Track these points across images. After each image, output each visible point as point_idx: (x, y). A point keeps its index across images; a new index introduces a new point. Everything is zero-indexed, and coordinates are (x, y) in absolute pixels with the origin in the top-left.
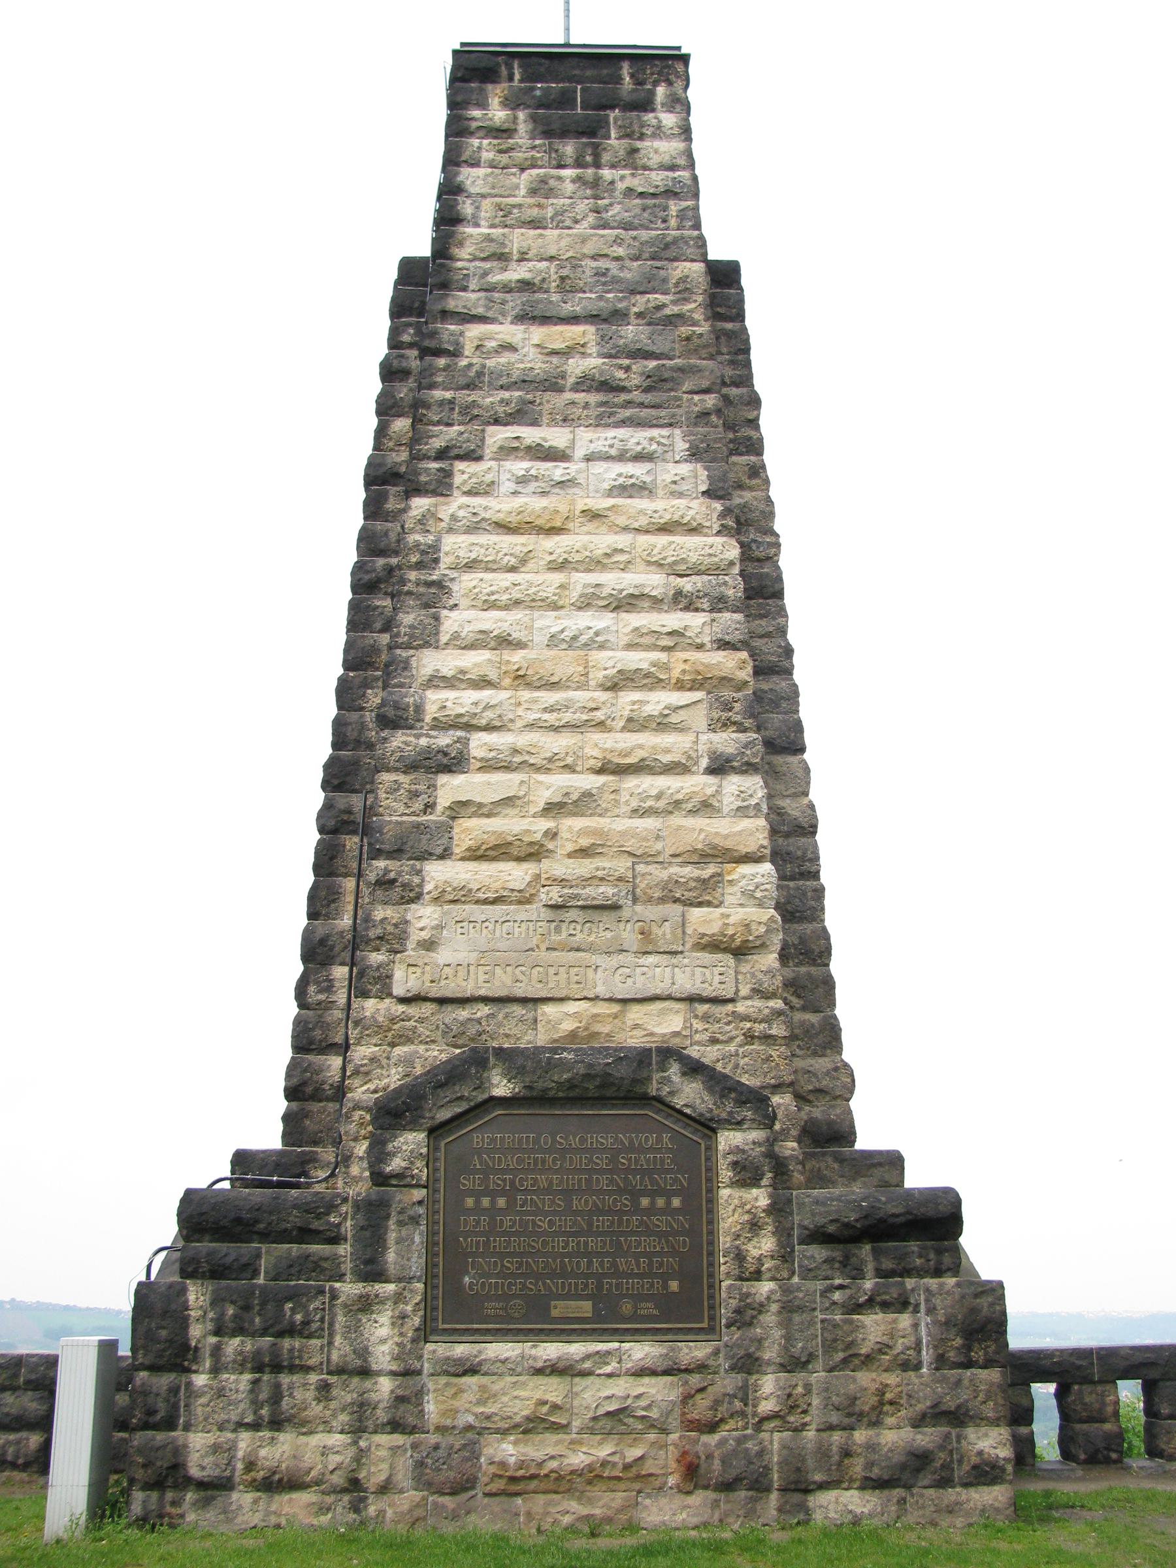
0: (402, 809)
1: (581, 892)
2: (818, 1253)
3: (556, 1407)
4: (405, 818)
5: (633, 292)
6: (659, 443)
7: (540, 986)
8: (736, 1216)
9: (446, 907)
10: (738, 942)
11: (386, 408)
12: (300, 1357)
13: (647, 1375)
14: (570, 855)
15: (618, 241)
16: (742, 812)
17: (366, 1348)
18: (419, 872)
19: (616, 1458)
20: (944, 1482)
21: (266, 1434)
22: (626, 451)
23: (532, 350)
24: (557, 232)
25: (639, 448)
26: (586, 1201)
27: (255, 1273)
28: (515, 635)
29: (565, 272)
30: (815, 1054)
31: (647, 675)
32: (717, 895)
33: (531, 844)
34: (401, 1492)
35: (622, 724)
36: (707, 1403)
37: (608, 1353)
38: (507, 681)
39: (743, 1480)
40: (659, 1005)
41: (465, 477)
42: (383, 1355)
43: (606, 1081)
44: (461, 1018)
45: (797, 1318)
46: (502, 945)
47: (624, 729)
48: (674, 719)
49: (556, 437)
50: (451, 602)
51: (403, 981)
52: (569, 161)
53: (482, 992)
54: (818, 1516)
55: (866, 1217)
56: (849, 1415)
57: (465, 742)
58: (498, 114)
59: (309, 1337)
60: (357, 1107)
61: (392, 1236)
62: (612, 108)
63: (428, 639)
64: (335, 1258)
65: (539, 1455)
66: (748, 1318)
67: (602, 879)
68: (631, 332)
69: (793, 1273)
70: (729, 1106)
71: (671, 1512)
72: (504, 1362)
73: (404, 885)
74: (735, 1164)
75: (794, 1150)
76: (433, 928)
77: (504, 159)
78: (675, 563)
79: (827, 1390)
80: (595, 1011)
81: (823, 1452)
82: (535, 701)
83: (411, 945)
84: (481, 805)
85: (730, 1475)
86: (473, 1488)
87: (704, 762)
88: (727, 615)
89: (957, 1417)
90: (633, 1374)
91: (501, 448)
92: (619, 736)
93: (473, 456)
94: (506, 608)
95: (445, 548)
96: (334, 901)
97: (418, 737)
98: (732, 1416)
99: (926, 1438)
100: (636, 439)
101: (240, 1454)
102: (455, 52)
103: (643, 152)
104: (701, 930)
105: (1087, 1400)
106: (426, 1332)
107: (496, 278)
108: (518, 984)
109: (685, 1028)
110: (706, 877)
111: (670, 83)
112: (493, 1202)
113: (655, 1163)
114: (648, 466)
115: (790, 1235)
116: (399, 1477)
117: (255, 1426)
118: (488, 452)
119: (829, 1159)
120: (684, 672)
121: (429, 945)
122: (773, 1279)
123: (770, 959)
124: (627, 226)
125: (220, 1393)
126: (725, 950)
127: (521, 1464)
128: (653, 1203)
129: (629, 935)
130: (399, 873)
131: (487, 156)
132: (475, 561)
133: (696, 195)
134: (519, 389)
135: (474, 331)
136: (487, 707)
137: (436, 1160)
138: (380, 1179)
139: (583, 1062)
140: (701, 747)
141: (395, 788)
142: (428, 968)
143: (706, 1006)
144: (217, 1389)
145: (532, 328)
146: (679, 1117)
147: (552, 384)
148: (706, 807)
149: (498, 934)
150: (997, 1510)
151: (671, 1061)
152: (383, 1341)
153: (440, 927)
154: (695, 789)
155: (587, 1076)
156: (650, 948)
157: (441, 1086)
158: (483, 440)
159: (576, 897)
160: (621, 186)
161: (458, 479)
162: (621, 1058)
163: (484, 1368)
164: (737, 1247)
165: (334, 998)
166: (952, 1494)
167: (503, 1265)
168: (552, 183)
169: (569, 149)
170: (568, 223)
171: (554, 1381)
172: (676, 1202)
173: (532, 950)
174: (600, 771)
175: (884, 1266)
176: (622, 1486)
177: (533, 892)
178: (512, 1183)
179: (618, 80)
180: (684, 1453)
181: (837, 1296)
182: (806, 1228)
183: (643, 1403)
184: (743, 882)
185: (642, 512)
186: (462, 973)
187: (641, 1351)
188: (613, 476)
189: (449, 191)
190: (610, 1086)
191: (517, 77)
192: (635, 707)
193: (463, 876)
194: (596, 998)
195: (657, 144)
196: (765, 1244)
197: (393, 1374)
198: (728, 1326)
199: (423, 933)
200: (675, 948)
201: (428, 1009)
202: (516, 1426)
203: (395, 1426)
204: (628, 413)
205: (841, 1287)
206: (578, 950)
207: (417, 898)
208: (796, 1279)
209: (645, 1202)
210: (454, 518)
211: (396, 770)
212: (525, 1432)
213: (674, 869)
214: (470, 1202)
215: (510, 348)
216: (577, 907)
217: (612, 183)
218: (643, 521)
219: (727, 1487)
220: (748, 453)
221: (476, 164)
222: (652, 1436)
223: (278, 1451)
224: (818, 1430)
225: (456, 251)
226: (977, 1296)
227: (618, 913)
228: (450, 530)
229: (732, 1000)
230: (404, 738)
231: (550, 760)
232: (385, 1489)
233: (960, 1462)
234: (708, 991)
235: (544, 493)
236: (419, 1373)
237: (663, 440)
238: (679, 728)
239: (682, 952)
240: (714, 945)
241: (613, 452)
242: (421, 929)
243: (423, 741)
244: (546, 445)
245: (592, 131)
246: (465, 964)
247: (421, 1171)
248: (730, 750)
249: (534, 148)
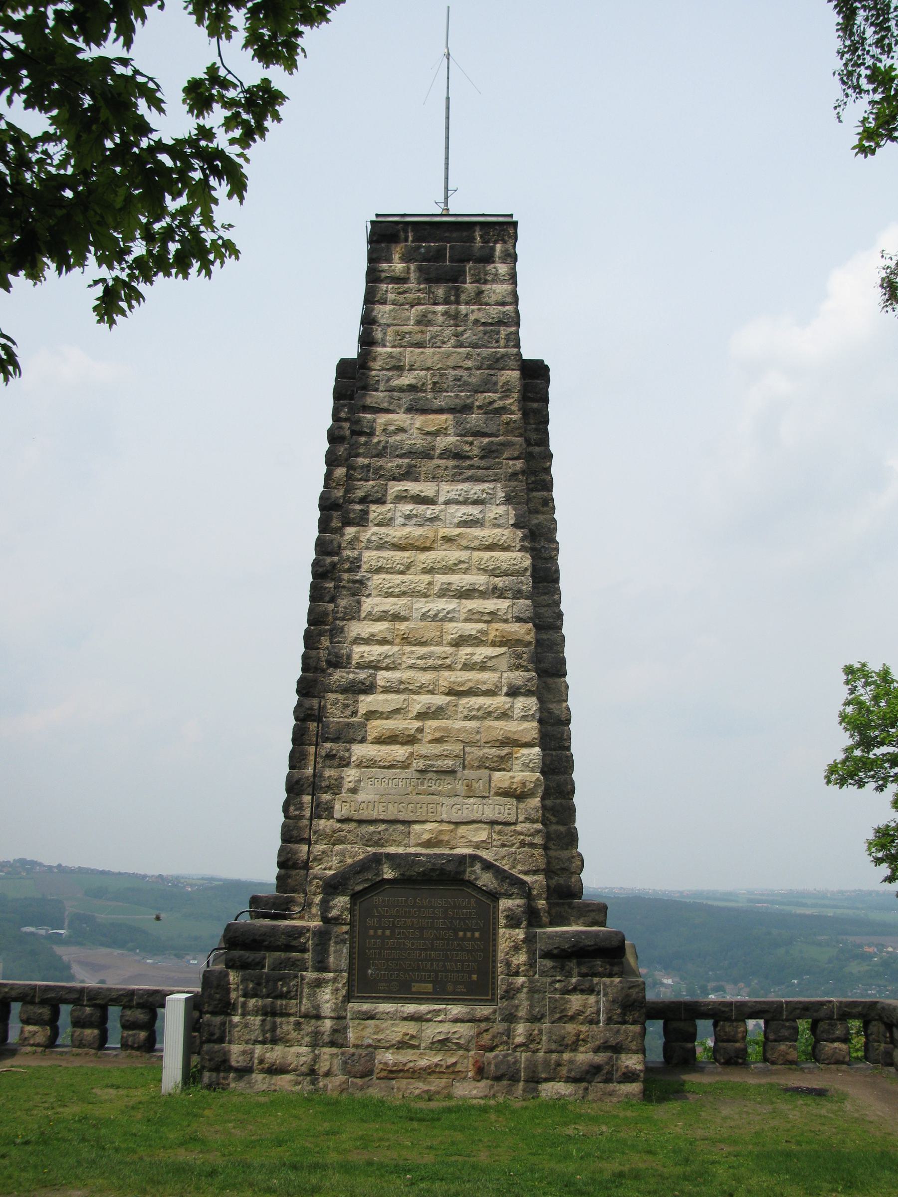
0: (339, 714)
2: (549, 963)
3: (413, 1037)
4: (341, 719)
5: (476, 392)
6: (487, 493)
11: (332, 460)
12: (286, 1009)
14: (430, 742)
15: (468, 357)
16: (524, 718)
17: (318, 1005)
18: (348, 750)
19: (442, 1063)
20: (608, 1080)
21: (269, 1046)
22: (468, 498)
23: (416, 431)
24: (432, 350)
25: (476, 497)
27: (263, 967)
28: (402, 613)
29: (436, 379)
30: (562, 848)
31: (476, 638)
34: (336, 1076)
35: (460, 666)
36: (489, 1037)
37: (440, 1010)
38: (398, 641)
39: (506, 1076)
40: (475, 826)
41: (376, 514)
42: (327, 1009)
43: (442, 872)
45: (536, 996)
46: (392, 792)
47: (461, 670)
48: (489, 664)
49: (427, 488)
50: (367, 593)
51: (340, 810)
52: (441, 300)
53: (381, 817)
54: (543, 1094)
55: (574, 946)
56: (561, 1045)
57: (374, 676)
58: (398, 267)
59: (291, 999)
60: (315, 877)
61: (332, 949)
62: (468, 261)
63: (353, 614)
64: (303, 959)
65: (404, 1060)
66: (511, 995)
67: (446, 756)
68: (475, 419)
70: (505, 886)
71: (470, 1090)
72: (387, 1013)
74: (507, 917)
76: (355, 782)
77: (401, 298)
78: (494, 569)
79: (550, 1032)
80: (441, 828)
81: (547, 1063)
82: (412, 652)
83: (344, 790)
84: (382, 713)
85: (498, 1074)
86: (371, 1075)
87: (505, 689)
88: (522, 601)
89: (617, 1049)
91: (397, 497)
92: (459, 673)
93: (381, 501)
94: (398, 596)
95: (364, 559)
96: (304, 759)
97: (348, 673)
98: (501, 1044)
99: (600, 1058)
100: (476, 490)
101: (256, 1056)
102: (372, 222)
103: (486, 293)
105: (727, 1030)
106: (348, 998)
107: (395, 383)
109: (488, 838)
111: (505, 242)
112: (383, 933)
114: (480, 507)
115: (534, 954)
116: (335, 1068)
117: (263, 1042)
118: (389, 498)
119: (566, 907)
120: (496, 636)
121: (354, 791)
122: (524, 976)
123: (536, 802)
124: (474, 346)
125: (246, 1026)
127: (395, 1064)
128: (465, 934)
129: (460, 787)
130: (338, 751)
131: (391, 296)
132: (381, 567)
133: (518, 324)
134: (408, 457)
135: (382, 419)
137: (354, 910)
138: (326, 920)
140: (504, 681)
141: (336, 702)
144: (245, 1023)
145: (416, 416)
147: (427, 454)
148: (505, 715)
150: (634, 1095)
152: (327, 1002)
153: (359, 781)
154: (500, 705)
155: (433, 870)
157: (358, 873)
158: (386, 491)
159: (433, 766)
160: (472, 317)
161: (372, 516)
163: (378, 1016)
164: (507, 959)
165: (304, 813)
166: (611, 1086)
168: (430, 316)
169: (440, 291)
170: (438, 344)
171: (412, 1023)
172: (477, 935)
174: (448, 694)
175: (582, 971)
176: (445, 1076)
178: (393, 922)
179: (473, 239)
180: (476, 1062)
181: (557, 985)
183: (456, 1036)
185: (476, 537)
186: (371, 807)
187: (456, 1010)
188: (460, 515)
189: (368, 320)
190: (445, 876)
191: (410, 239)
194: (442, 821)
195: (494, 286)
196: (521, 958)
197: (332, 1018)
198: (501, 999)
199: (350, 784)
200: (485, 794)
201: (352, 825)
202: (393, 1045)
203: (332, 1044)
204: (470, 473)
205: (559, 981)
206: (433, 794)
207: (347, 765)
208: (537, 976)
209: (461, 934)
210: (369, 541)
211: (336, 692)
212: (398, 1048)
213: (486, 750)
214: (372, 932)
215: (401, 430)
217: (466, 315)
218: (476, 543)
219: (498, 1079)
220: (542, 490)
221: (384, 303)
222: (461, 1052)
223: (275, 1054)
224: (545, 1052)
225: (371, 364)
226: (630, 988)
228: (367, 548)
229: (515, 824)
230: (340, 674)
231: (420, 687)
232: (327, 1074)
233: (617, 1070)
234: (501, 818)
235: (420, 525)
236: (345, 1018)
237: (490, 491)
238: (492, 669)
241: (461, 499)
243: (351, 676)
244: (422, 494)
245: (455, 278)
247: (347, 916)
248: (520, 683)
249: (419, 290)
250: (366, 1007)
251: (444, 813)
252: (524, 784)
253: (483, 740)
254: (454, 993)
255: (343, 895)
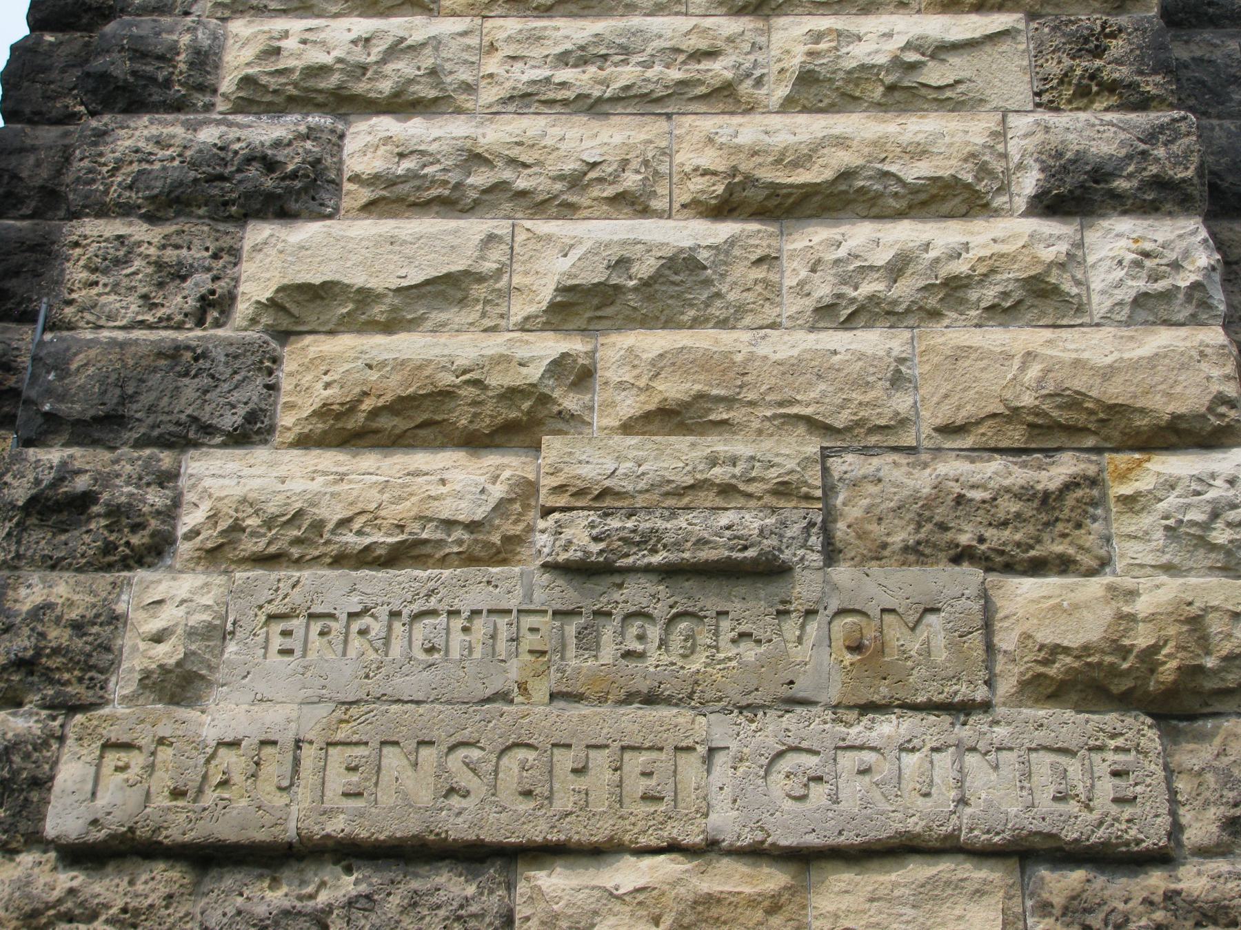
0: (132, 308)
1: (660, 524)
4: (137, 334)
7: (525, 806)
9: (240, 575)
10: (1169, 669)
14: (627, 428)
16: (1148, 308)
18: (166, 479)
32: (1090, 541)
33: (511, 394)
35: (782, 91)
40: (917, 871)
44: (261, 910)
46: (411, 683)
47: (788, 105)
48: (935, 75)
51: (82, 792)
53: (337, 826)
67: (727, 490)
73: (116, 513)
76: (191, 633)
83: (122, 684)
84: (365, 296)
87: (1029, 183)
92: (776, 121)
97: (194, 127)
104: (1047, 636)
108: (455, 801)
110: (1053, 486)
121: (180, 685)
126: (1126, 701)
129: (814, 654)
130: (104, 479)
136: (397, 49)
140: (1014, 148)
141: (118, 257)
142: (165, 754)
143: (1076, 877)
148: (1042, 296)
149: (397, 649)
153: (217, 633)
156: (882, 692)
159: (649, 540)
173: (504, 697)
174: (722, 209)
177: (518, 529)
184: (1171, 501)
186: (275, 766)
192: (823, 46)
193: (297, 485)
194: (709, 849)
199: (161, 650)
200: (963, 691)
201: (155, 882)
206: (651, 699)
207: (156, 551)
211: (125, 210)
213: (951, 467)
216: (648, 570)
227: (777, 589)
229: (1162, 858)
231: (575, 181)
234: (1077, 825)
238: (948, 100)
239: (986, 706)
240: (1087, 682)
242: (158, 638)
243: (208, 135)
246: (287, 738)
251: (717, 799)
252: (1196, 623)
253: (930, 418)
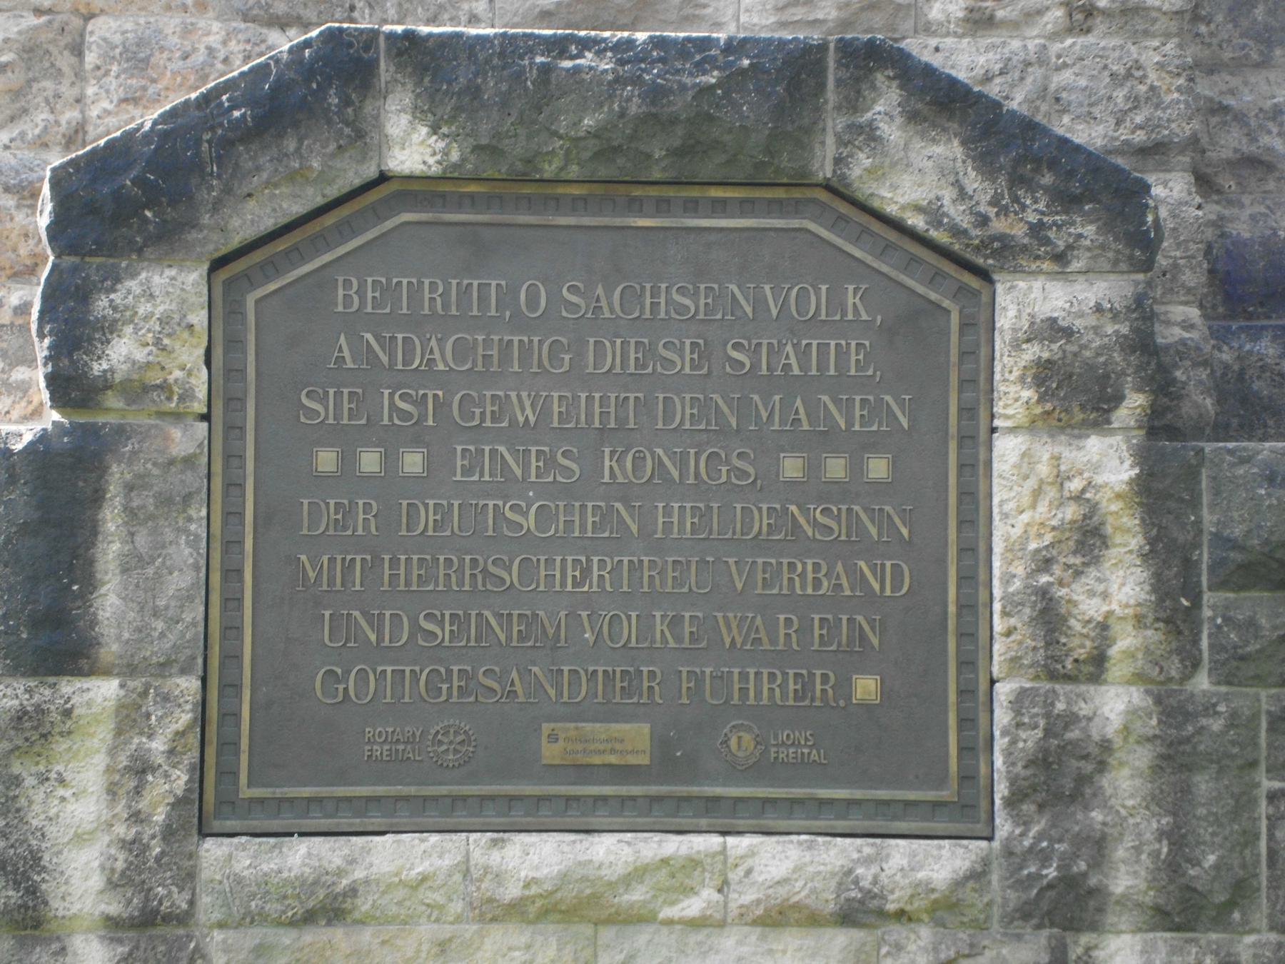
8: (1042, 508)
13: (799, 924)
17: (35, 860)
26: (638, 460)
37: (693, 863)
61: (110, 551)
69: (1196, 665)
75: (1188, 326)
90: (758, 922)
106: (202, 815)
113: (822, 366)
139: (636, 81)
146: (892, 236)
151: (879, 77)
152: (80, 839)
162: (743, 72)
163: (364, 905)
164: (1044, 593)
167: (416, 628)
172: (878, 468)
182: (1234, 545)
187: (778, 861)
196: (1117, 589)
208: (1202, 682)
236: (184, 919)
250: (299, 857)
254: (758, 770)
255: (162, 260)
